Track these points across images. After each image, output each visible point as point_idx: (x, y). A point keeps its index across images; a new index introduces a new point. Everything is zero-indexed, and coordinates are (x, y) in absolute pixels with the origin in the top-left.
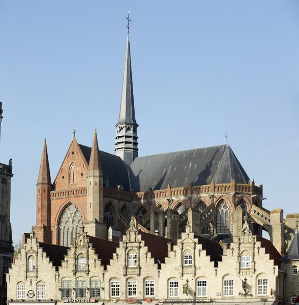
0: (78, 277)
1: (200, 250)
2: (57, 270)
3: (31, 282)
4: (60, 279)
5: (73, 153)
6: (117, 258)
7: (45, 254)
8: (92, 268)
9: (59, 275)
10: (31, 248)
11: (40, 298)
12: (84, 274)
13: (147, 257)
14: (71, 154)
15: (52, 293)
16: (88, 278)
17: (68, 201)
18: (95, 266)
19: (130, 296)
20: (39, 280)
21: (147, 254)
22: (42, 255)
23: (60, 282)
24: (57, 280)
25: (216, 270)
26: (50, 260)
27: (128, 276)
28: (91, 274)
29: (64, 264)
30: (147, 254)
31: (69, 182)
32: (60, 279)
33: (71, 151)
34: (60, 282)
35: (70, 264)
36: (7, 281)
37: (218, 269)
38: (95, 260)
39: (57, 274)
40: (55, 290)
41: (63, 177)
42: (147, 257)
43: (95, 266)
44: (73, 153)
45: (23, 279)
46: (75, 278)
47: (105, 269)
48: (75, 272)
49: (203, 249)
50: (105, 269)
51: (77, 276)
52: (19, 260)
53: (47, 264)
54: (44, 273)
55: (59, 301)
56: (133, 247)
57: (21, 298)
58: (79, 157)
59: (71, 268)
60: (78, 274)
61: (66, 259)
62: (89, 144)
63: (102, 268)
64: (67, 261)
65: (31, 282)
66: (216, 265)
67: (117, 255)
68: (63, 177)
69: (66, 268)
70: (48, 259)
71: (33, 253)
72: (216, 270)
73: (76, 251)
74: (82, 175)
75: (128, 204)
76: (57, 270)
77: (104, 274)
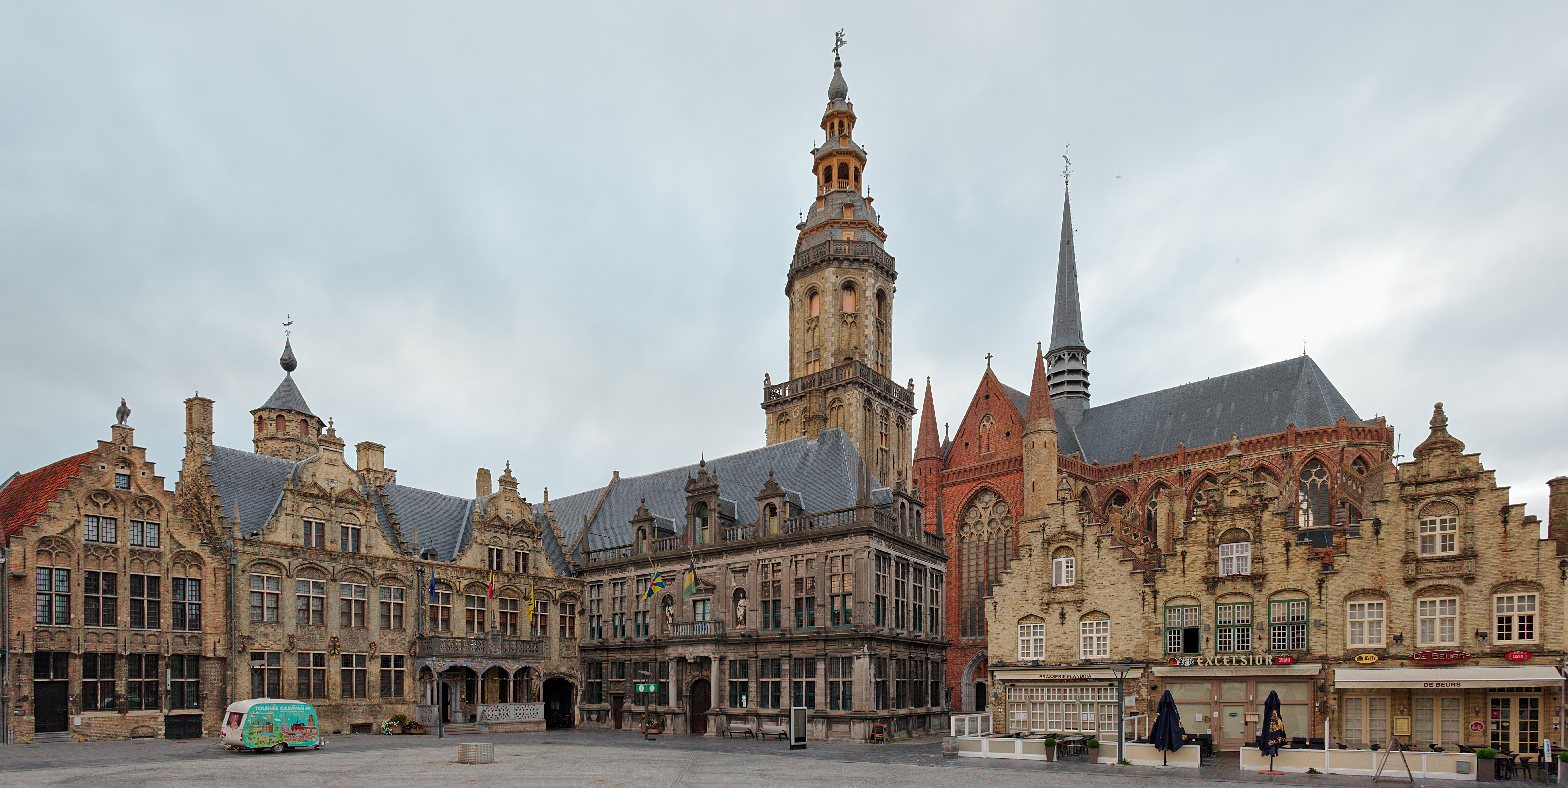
0: (1222, 596)
4: (1160, 603)
7: (1106, 542)
9: (1155, 593)
11: (1095, 656)
15: (1134, 643)
18: (1288, 562)
22: (1098, 542)
23: (1160, 610)
28: (1273, 585)
35: (1194, 562)
36: (989, 615)
38: (1287, 545)
39: (1147, 590)
40: (1140, 635)
43: (1288, 562)
46: (1213, 598)
48: (1212, 583)
51: (1219, 592)
52: (1026, 561)
53: (1116, 566)
54: (1104, 591)
55: (1157, 663)
56: (1443, 494)
57: (1032, 658)
59: (1197, 572)
63: (1315, 567)
64: (1184, 553)
69: (1179, 572)
71: (1067, 539)
75: (1090, 486)
77: (1320, 583)
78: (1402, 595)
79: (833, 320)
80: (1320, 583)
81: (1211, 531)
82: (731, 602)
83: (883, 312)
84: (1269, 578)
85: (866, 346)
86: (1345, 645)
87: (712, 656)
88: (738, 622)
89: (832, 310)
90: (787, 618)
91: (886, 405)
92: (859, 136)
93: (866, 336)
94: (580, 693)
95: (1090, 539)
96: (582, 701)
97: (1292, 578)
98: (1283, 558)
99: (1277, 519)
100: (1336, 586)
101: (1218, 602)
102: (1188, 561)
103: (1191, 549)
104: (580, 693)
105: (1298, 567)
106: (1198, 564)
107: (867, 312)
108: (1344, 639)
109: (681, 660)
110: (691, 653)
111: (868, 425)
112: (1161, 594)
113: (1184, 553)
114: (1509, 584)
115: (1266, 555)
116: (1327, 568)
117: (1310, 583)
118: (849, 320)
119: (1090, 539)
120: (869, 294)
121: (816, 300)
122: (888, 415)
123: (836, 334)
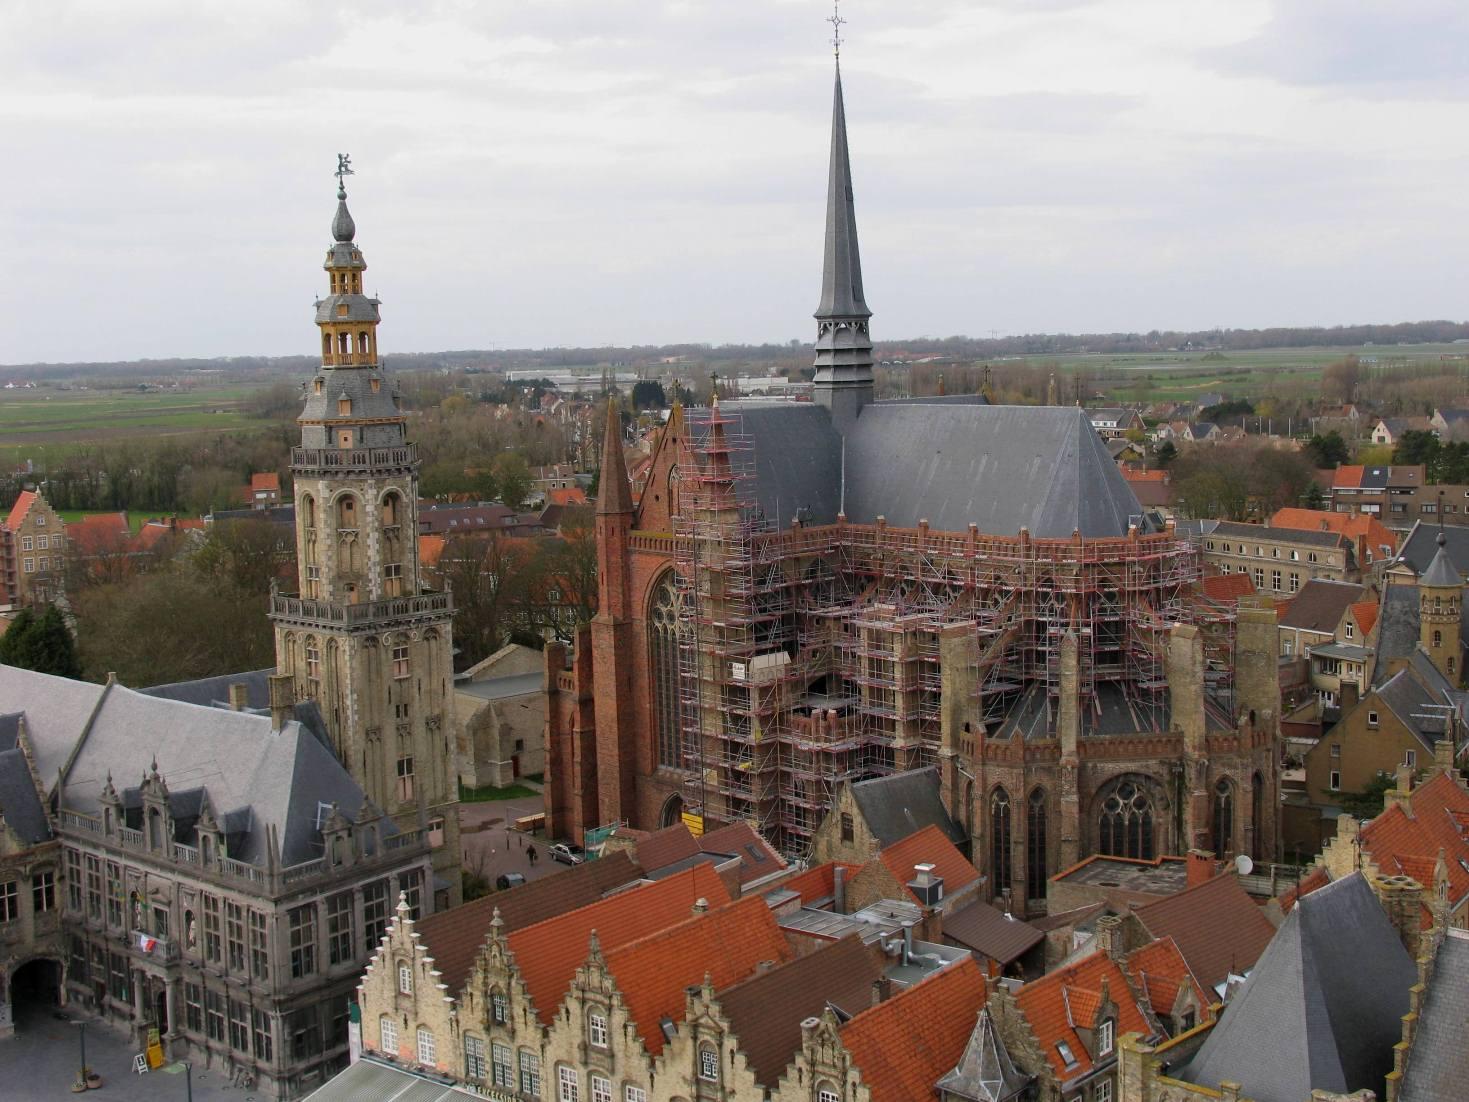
1: (732, 1052)
5: (674, 440)
14: (670, 442)
18: (526, 1023)
20: (419, 1022)
24: (455, 1033)
27: (592, 1067)
28: (519, 1041)
30: (625, 1027)
31: (671, 514)
32: (461, 1032)
38: (525, 1010)
41: (657, 498)
43: (526, 1023)
44: (674, 440)
45: (390, 1010)
47: (546, 1034)
49: (740, 1049)
50: (546, 1034)
65: (406, 1021)
67: (567, 1011)
68: (657, 498)
73: (486, 978)
77: (543, 1047)
80: (543, 1047)
81: (485, 984)
83: (398, 514)
85: (370, 569)
91: (402, 629)
92: (369, 287)
93: (369, 558)
94: (65, 970)
96: (68, 979)
104: (65, 970)
105: (531, 1029)
107: (368, 530)
111: (373, 665)
117: (537, 1047)
118: (350, 539)
120: (370, 508)
122: (407, 637)
123: (334, 558)
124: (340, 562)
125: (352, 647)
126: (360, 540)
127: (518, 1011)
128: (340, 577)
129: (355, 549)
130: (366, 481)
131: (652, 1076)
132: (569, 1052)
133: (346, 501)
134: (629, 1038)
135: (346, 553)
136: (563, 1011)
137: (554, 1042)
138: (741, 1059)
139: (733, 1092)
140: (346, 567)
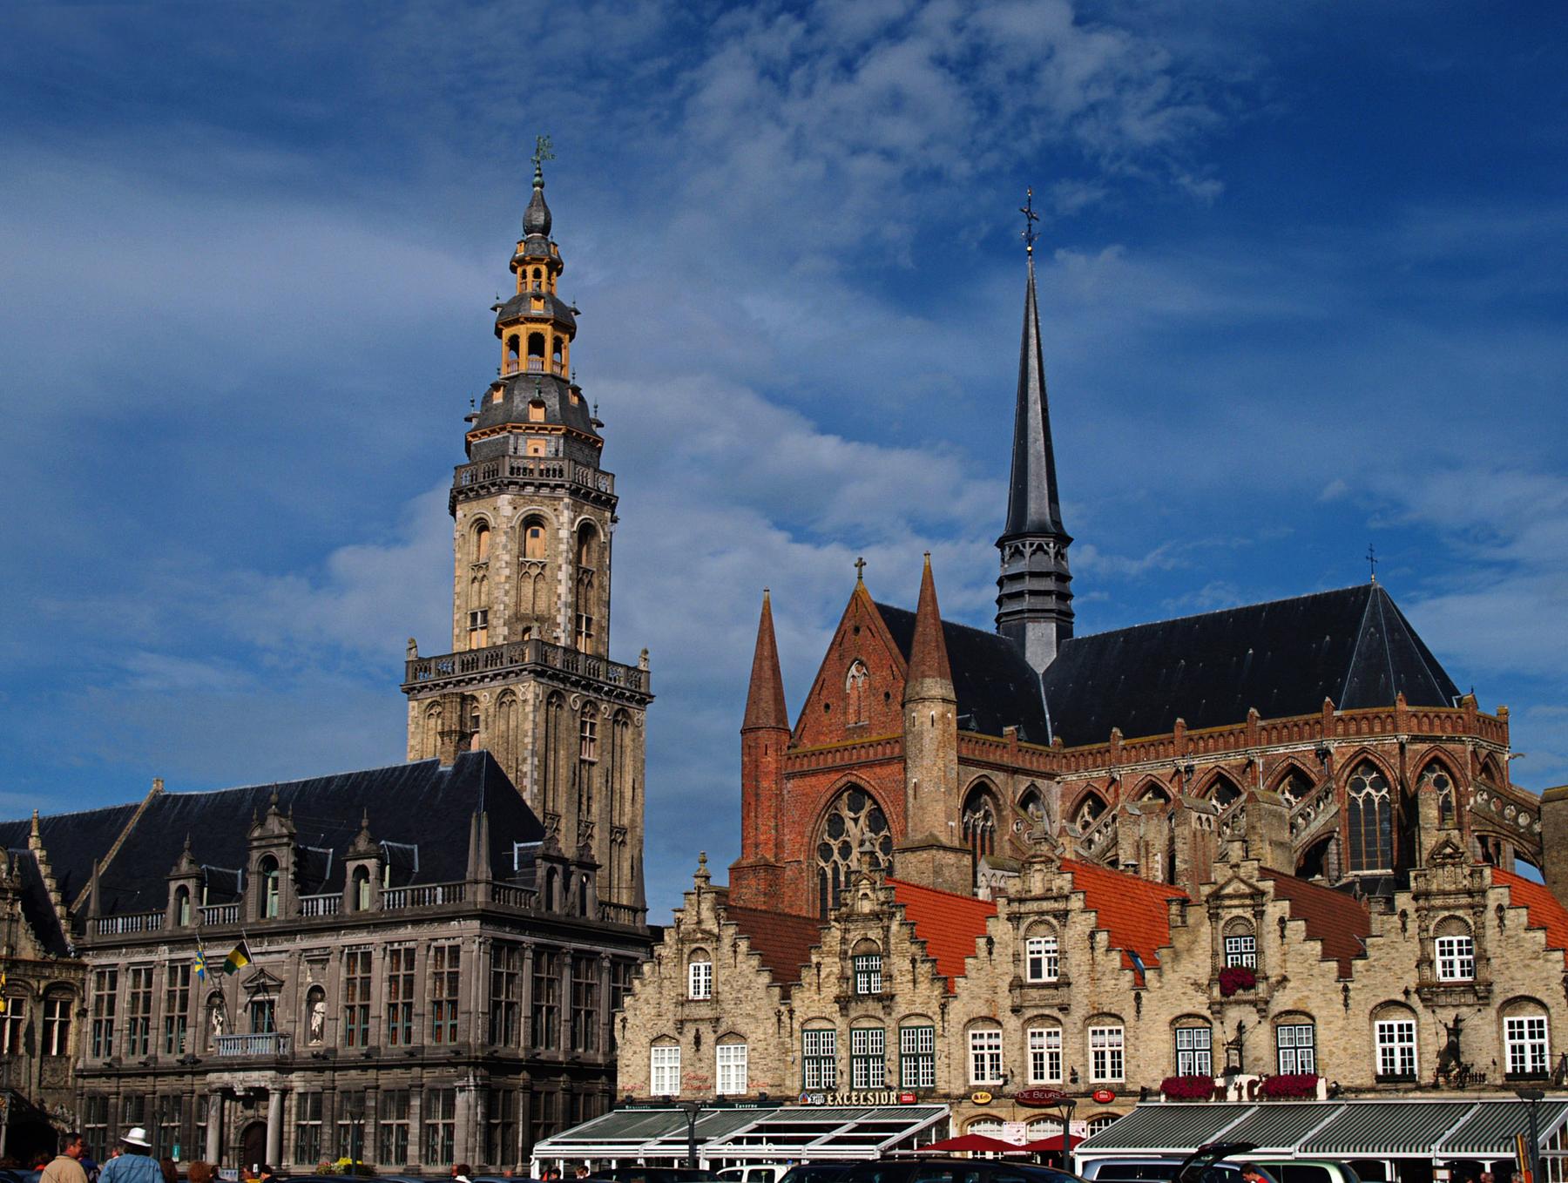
2: (786, 996)
3: (698, 1041)
4: (796, 1026)
6: (990, 953)
7: (743, 946)
8: (902, 987)
9: (791, 1012)
10: (699, 922)
12: (874, 1008)
13: (1092, 948)
14: (850, 635)
16: (890, 1023)
17: (845, 779)
18: (914, 981)
19: (1039, 1082)
21: (1092, 936)
22: (735, 945)
23: (797, 1034)
25: (1346, 989)
26: (763, 964)
28: (901, 1008)
29: (807, 976)
30: (1092, 936)
32: (796, 1026)
33: (849, 625)
34: (797, 1034)
35: (828, 976)
37: (1350, 986)
38: (913, 961)
39: (783, 1008)
41: (827, 706)
42: (1092, 948)
43: (914, 981)
44: (857, 630)
51: (853, 1014)
58: (881, 640)
60: (856, 1010)
61: (814, 959)
62: (906, 599)
64: (818, 965)
65: (698, 1041)
66: (1345, 973)
67: (990, 942)
68: (827, 706)
69: (814, 988)
70: (755, 962)
72: (1346, 989)
74: (887, 695)
76: (786, 996)
77: (943, 1007)
78: (1012, 1023)
79: (507, 572)
80: (943, 1007)
81: (844, 941)
82: (304, 1006)
84: (898, 999)
86: (967, 1081)
87: (270, 1087)
88: (315, 1036)
89: (507, 557)
90: (378, 1031)
91: (592, 695)
93: (559, 596)
95: (727, 943)
97: (919, 1001)
98: (910, 977)
99: (905, 930)
100: (959, 1010)
101: (855, 1025)
102: (823, 975)
103: (827, 960)
105: (924, 986)
106: (833, 979)
108: (965, 1074)
109: (227, 1093)
110: (239, 1081)
112: (797, 1013)
113: (818, 965)
114: (1100, 1015)
115: (895, 973)
116: (949, 992)
117: (934, 1008)
119: (727, 943)
121: (485, 534)
123: (513, 593)
124: (518, 604)
125: (537, 696)
126: (547, 572)
127: (900, 964)
128: (518, 617)
129: (540, 585)
130: (561, 499)
131: (1138, 997)
132: (990, 1002)
133: (533, 522)
134: (1100, 951)
135: (528, 588)
136: (982, 942)
137: (965, 997)
138: (1297, 928)
139: (1285, 979)
140: (526, 608)
